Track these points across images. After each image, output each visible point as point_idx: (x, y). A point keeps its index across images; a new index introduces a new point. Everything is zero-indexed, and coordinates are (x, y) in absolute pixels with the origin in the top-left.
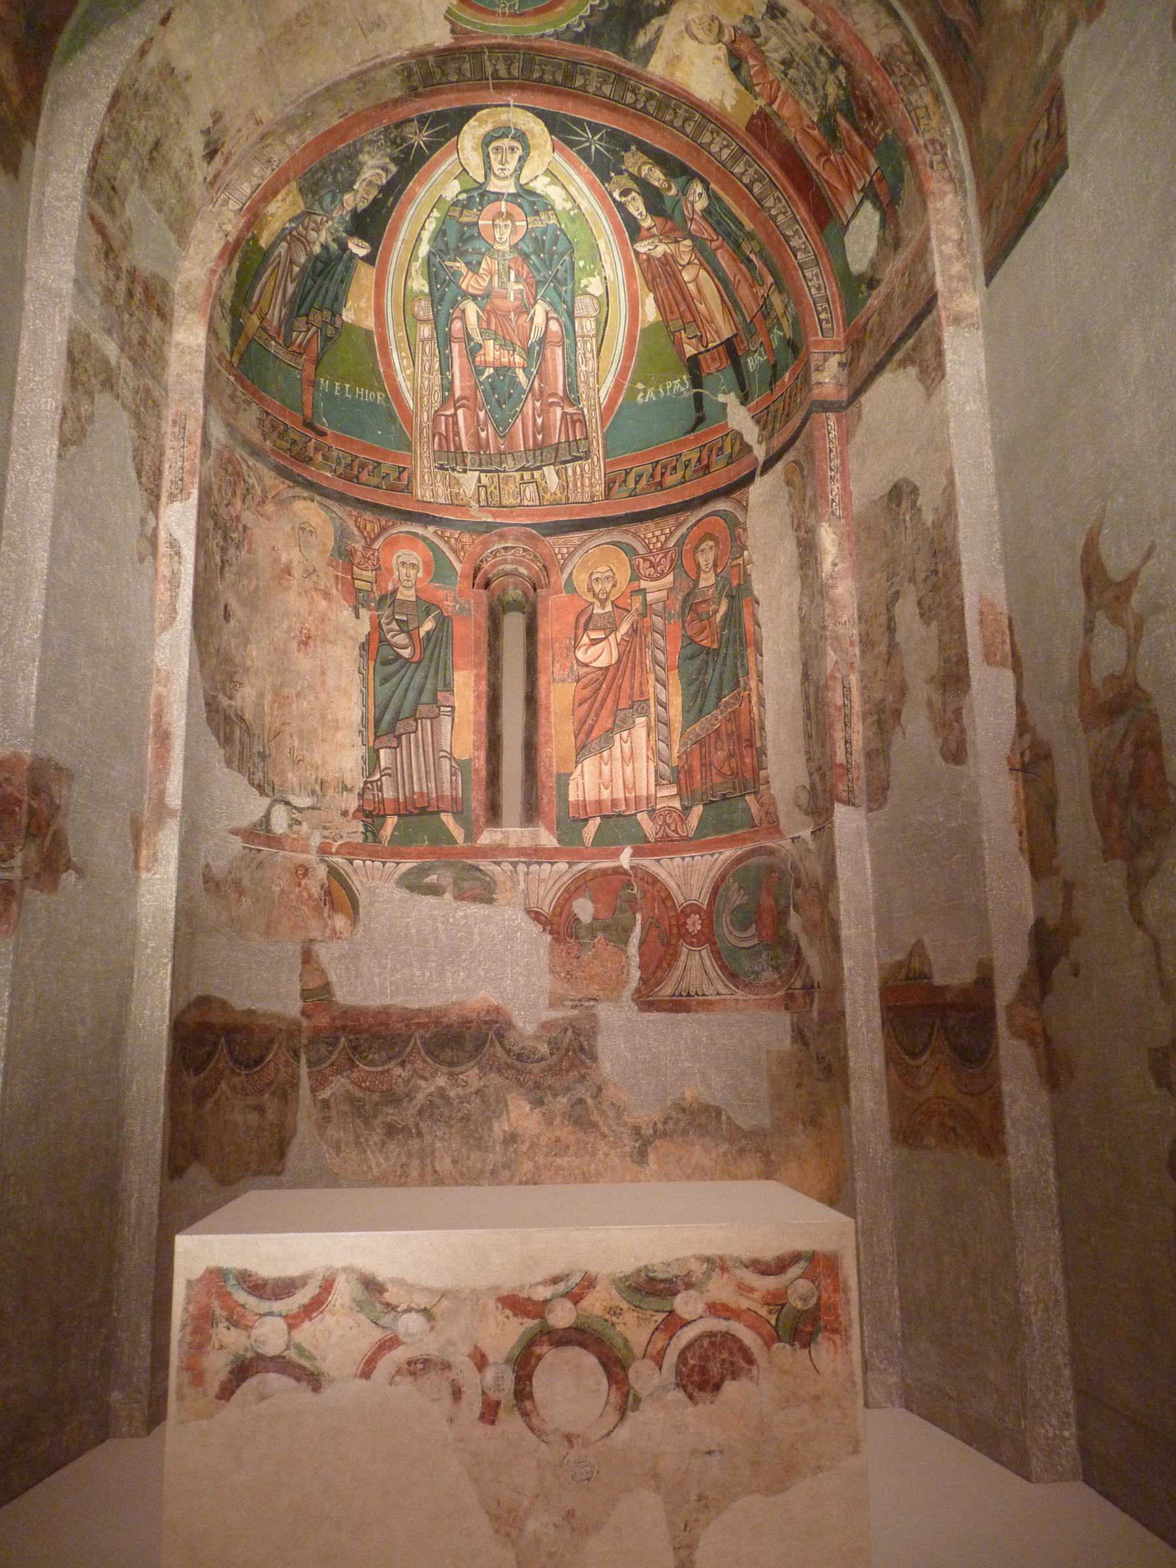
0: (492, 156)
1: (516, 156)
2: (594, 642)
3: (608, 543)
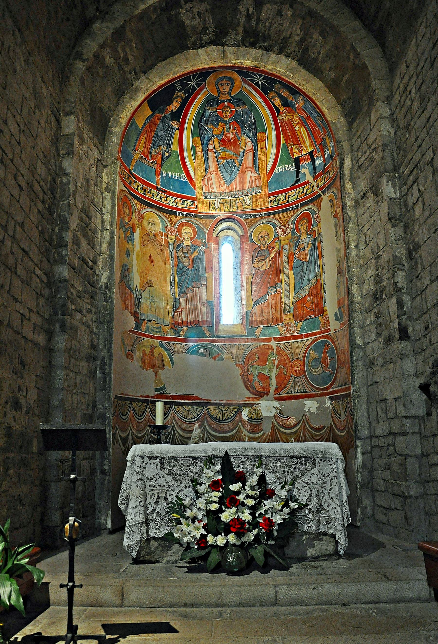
0: (220, 87)
1: (229, 87)
2: (260, 261)
3: (266, 222)
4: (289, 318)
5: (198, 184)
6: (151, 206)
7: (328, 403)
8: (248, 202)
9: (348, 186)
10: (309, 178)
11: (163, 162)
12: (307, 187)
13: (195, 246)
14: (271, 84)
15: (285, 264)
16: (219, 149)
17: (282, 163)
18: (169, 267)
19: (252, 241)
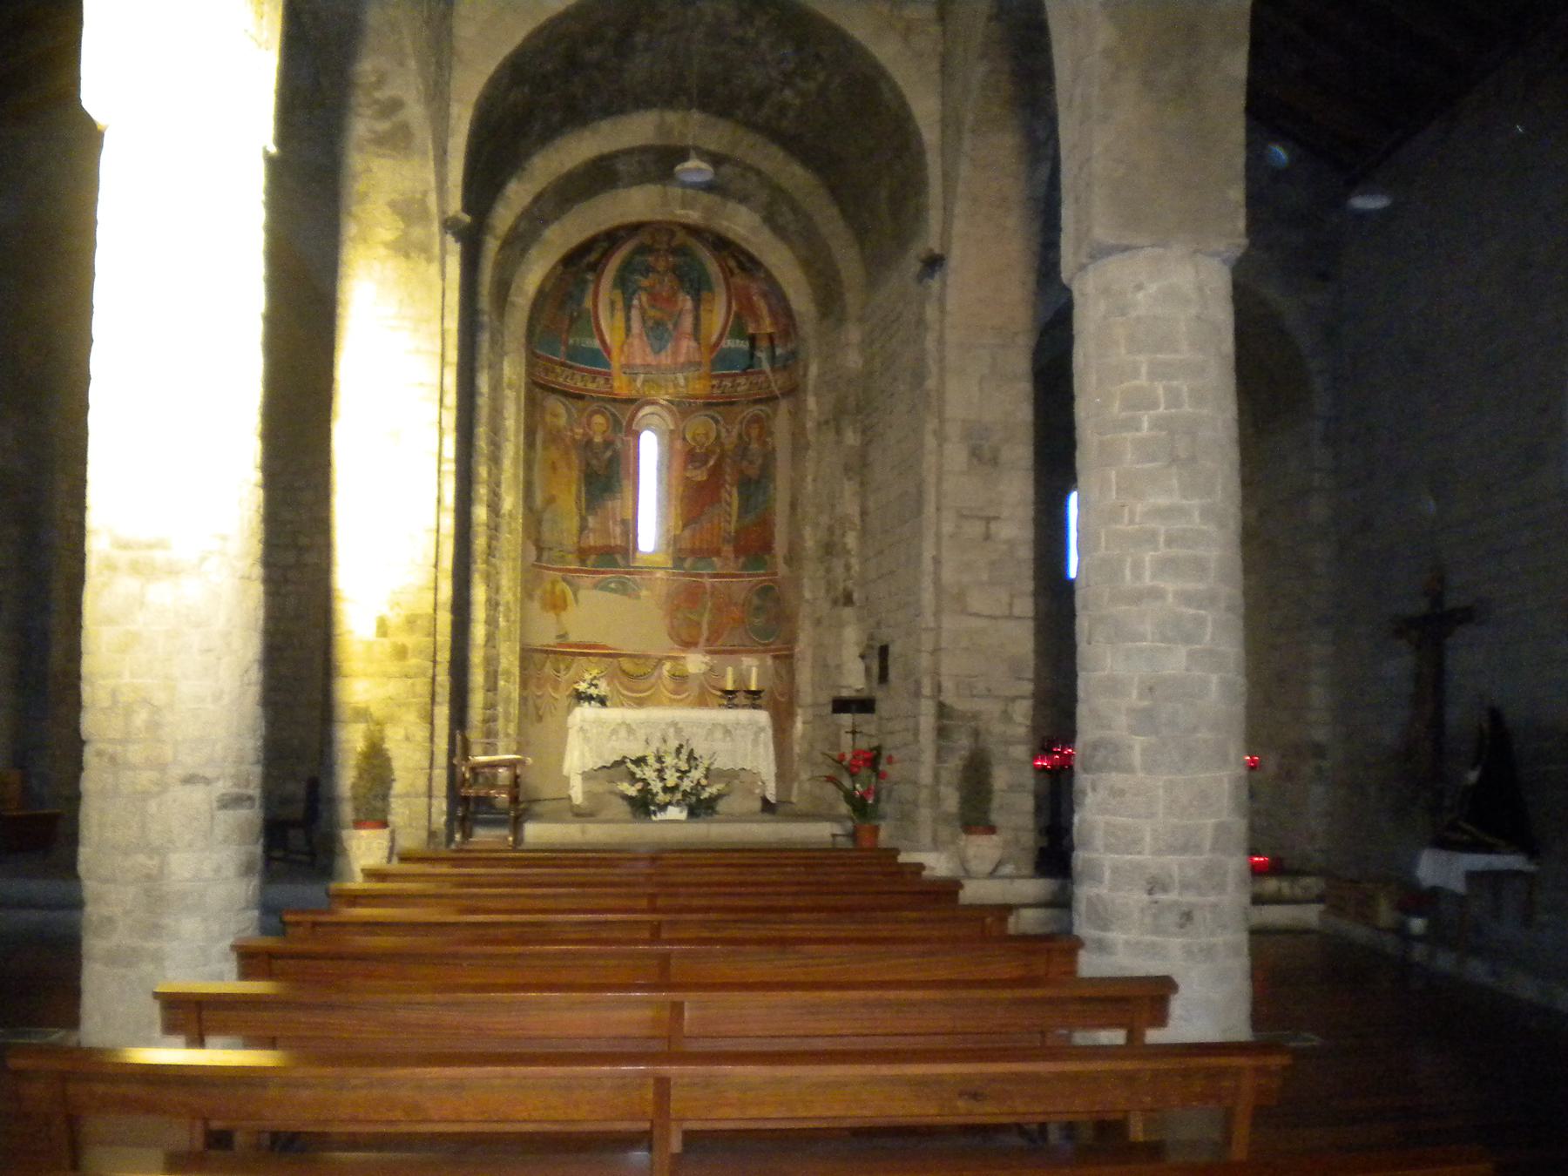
4: (728, 549)
5: (615, 352)
6: (554, 391)
7: (769, 662)
8: (682, 382)
9: (812, 403)
10: (766, 366)
11: (570, 326)
12: (762, 378)
13: (608, 444)
14: (722, 245)
15: (728, 478)
16: (646, 305)
17: (733, 336)
18: (575, 474)
19: (684, 439)
